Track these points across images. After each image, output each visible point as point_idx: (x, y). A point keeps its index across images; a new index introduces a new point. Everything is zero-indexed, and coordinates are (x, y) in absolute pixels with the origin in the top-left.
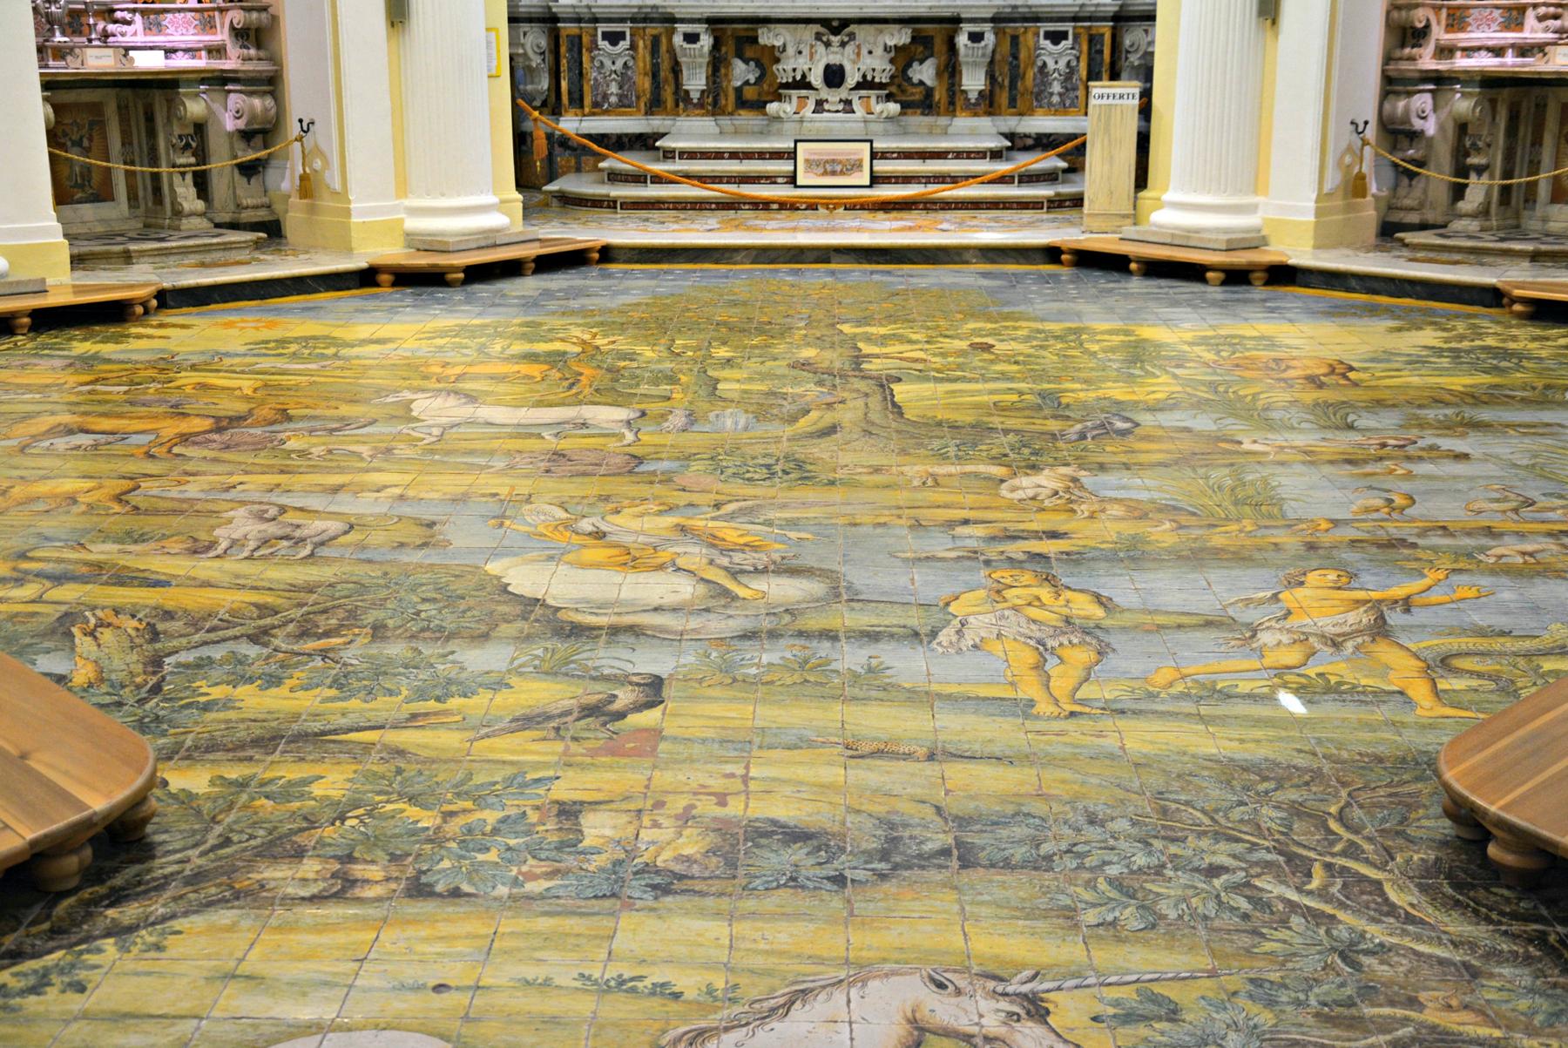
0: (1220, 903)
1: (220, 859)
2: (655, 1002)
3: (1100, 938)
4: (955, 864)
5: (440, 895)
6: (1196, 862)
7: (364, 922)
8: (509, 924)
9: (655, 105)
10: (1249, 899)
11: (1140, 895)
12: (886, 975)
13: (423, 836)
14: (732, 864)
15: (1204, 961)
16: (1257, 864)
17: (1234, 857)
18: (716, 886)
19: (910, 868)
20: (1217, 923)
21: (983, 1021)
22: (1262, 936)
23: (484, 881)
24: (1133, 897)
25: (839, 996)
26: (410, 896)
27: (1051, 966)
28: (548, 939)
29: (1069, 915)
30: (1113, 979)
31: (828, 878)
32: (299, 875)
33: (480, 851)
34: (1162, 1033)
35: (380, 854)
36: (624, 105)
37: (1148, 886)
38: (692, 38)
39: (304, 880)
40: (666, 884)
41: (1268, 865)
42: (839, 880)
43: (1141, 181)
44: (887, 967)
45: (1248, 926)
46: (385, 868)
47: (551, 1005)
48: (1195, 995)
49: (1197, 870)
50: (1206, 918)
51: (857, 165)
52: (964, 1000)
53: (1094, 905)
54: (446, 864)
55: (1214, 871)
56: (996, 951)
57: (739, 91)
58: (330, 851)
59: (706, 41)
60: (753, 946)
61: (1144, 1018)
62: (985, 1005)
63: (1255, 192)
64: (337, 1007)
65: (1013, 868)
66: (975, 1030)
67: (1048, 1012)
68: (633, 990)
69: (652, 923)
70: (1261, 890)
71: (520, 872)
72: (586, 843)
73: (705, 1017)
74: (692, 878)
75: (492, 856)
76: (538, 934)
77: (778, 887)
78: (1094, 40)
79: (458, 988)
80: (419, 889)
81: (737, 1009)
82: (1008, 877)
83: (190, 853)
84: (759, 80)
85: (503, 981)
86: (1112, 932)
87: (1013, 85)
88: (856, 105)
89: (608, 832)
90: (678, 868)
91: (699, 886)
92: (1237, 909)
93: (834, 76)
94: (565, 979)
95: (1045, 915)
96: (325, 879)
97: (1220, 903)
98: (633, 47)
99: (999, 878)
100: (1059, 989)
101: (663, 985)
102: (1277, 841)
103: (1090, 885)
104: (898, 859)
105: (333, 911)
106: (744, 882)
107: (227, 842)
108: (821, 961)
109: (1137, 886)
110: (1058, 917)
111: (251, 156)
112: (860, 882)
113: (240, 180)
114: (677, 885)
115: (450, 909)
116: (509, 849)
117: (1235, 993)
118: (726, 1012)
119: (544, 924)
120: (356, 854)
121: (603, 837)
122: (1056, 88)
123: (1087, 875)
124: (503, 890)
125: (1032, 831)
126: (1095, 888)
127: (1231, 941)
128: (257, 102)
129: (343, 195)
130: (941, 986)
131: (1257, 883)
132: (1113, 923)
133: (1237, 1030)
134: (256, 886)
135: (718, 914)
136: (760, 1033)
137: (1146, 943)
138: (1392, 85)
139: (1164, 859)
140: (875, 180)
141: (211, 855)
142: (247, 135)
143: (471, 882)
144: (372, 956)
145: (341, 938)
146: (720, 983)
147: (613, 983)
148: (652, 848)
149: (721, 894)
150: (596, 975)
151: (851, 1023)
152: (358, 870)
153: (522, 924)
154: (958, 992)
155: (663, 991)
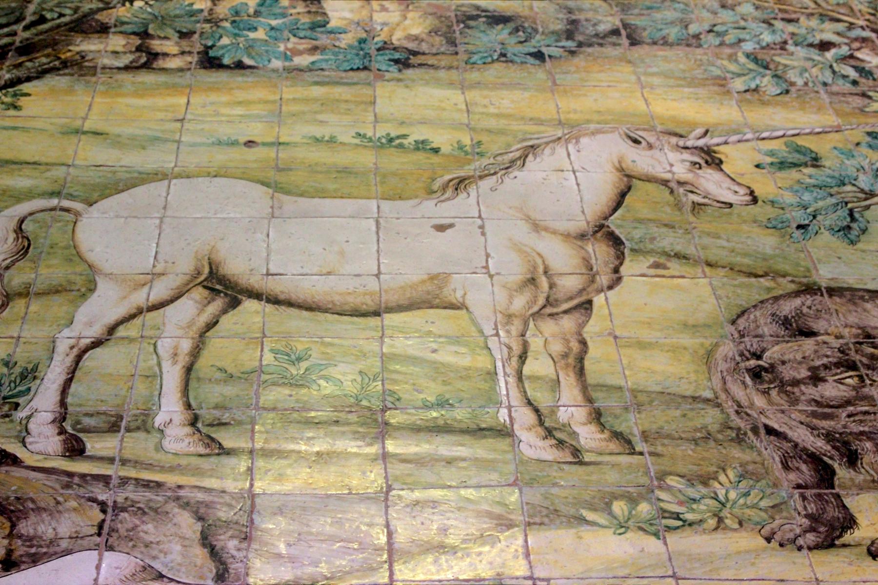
0: (834, 72)
1: (41, 33)
2: (420, 156)
3: (749, 102)
4: (625, 41)
5: (228, 67)
6: (810, 40)
7: (174, 88)
8: (289, 92)
10: (855, 68)
11: (772, 66)
12: (593, 134)
13: (201, 17)
14: (452, 42)
15: (831, 119)
16: (856, 39)
17: (838, 34)
18: (444, 61)
19: (590, 45)
20: (835, 89)
21: (674, 169)
22: (870, 97)
23: (260, 55)
24: (767, 67)
25: (561, 151)
26: (205, 68)
27: (717, 125)
28: (326, 104)
29: (721, 83)
30: (764, 135)
31: (531, 54)
32: (110, 48)
33: (249, 29)
34: (810, 177)
35: (170, 32)
37: (777, 59)
39: (115, 53)
40: (405, 59)
41: (864, 40)
42: (539, 56)
44: (592, 126)
45: (857, 90)
46: (177, 44)
47: (342, 158)
48: (828, 146)
49: (811, 45)
50: (825, 84)
52: (656, 153)
53: (739, 75)
54: (225, 41)
55: (824, 46)
56: (672, 113)
58: (128, 28)
60: (485, 110)
61: (795, 165)
62: (674, 156)
64: (173, 158)
65: (671, 45)
66: (668, 176)
67: (721, 162)
68: (401, 146)
69: (401, 92)
70: (862, 61)
71: (287, 49)
72: (333, 24)
73: (461, 167)
74: (424, 54)
75: (260, 34)
76: (315, 100)
77: (493, 61)
79: (264, 144)
80: (210, 62)
81: (485, 161)
82: (668, 52)
83: (14, 27)
85: (297, 139)
86: (756, 96)
89: (348, 15)
90: (412, 46)
91: (431, 61)
92: (847, 77)
94: (346, 137)
95: (702, 83)
96: (131, 52)
97: (834, 72)
99: (661, 53)
100: (726, 143)
101: (423, 142)
102: (868, 20)
103: (732, 58)
104: (580, 38)
105: (146, 78)
106: (465, 57)
107: (42, 20)
108: (540, 122)
109: (768, 60)
110: (714, 85)
112: (556, 58)
114: (413, 60)
115: (240, 79)
116: (272, 28)
117: (858, 144)
118: (477, 163)
119: (317, 91)
120: (151, 31)
121: (345, 19)
123: (728, 51)
124: (277, 64)
125: (680, 15)
126: (736, 61)
127: (848, 103)
130: (636, 142)
131: (858, 55)
132: (756, 90)
133: (865, 173)
134: (78, 57)
135: (451, 84)
136: (507, 180)
137: (785, 105)
139: (785, 36)
141: (33, 31)
143: (249, 56)
144: (189, 116)
145: (160, 102)
146: (467, 141)
147: (384, 141)
148: (386, 29)
149: (450, 68)
150: (370, 134)
151: (574, 172)
152: (157, 45)
153: (300, 92)
154: (650, 146)
155: (421, 146)
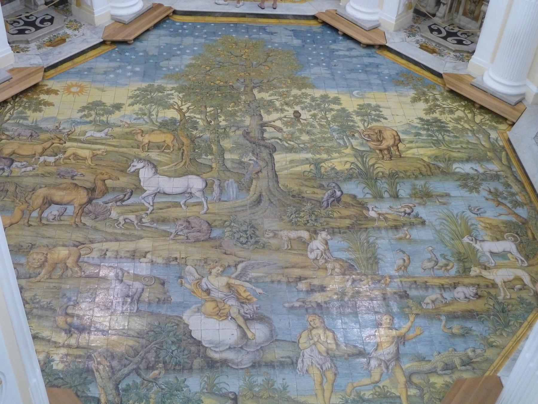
129: (91, 7)
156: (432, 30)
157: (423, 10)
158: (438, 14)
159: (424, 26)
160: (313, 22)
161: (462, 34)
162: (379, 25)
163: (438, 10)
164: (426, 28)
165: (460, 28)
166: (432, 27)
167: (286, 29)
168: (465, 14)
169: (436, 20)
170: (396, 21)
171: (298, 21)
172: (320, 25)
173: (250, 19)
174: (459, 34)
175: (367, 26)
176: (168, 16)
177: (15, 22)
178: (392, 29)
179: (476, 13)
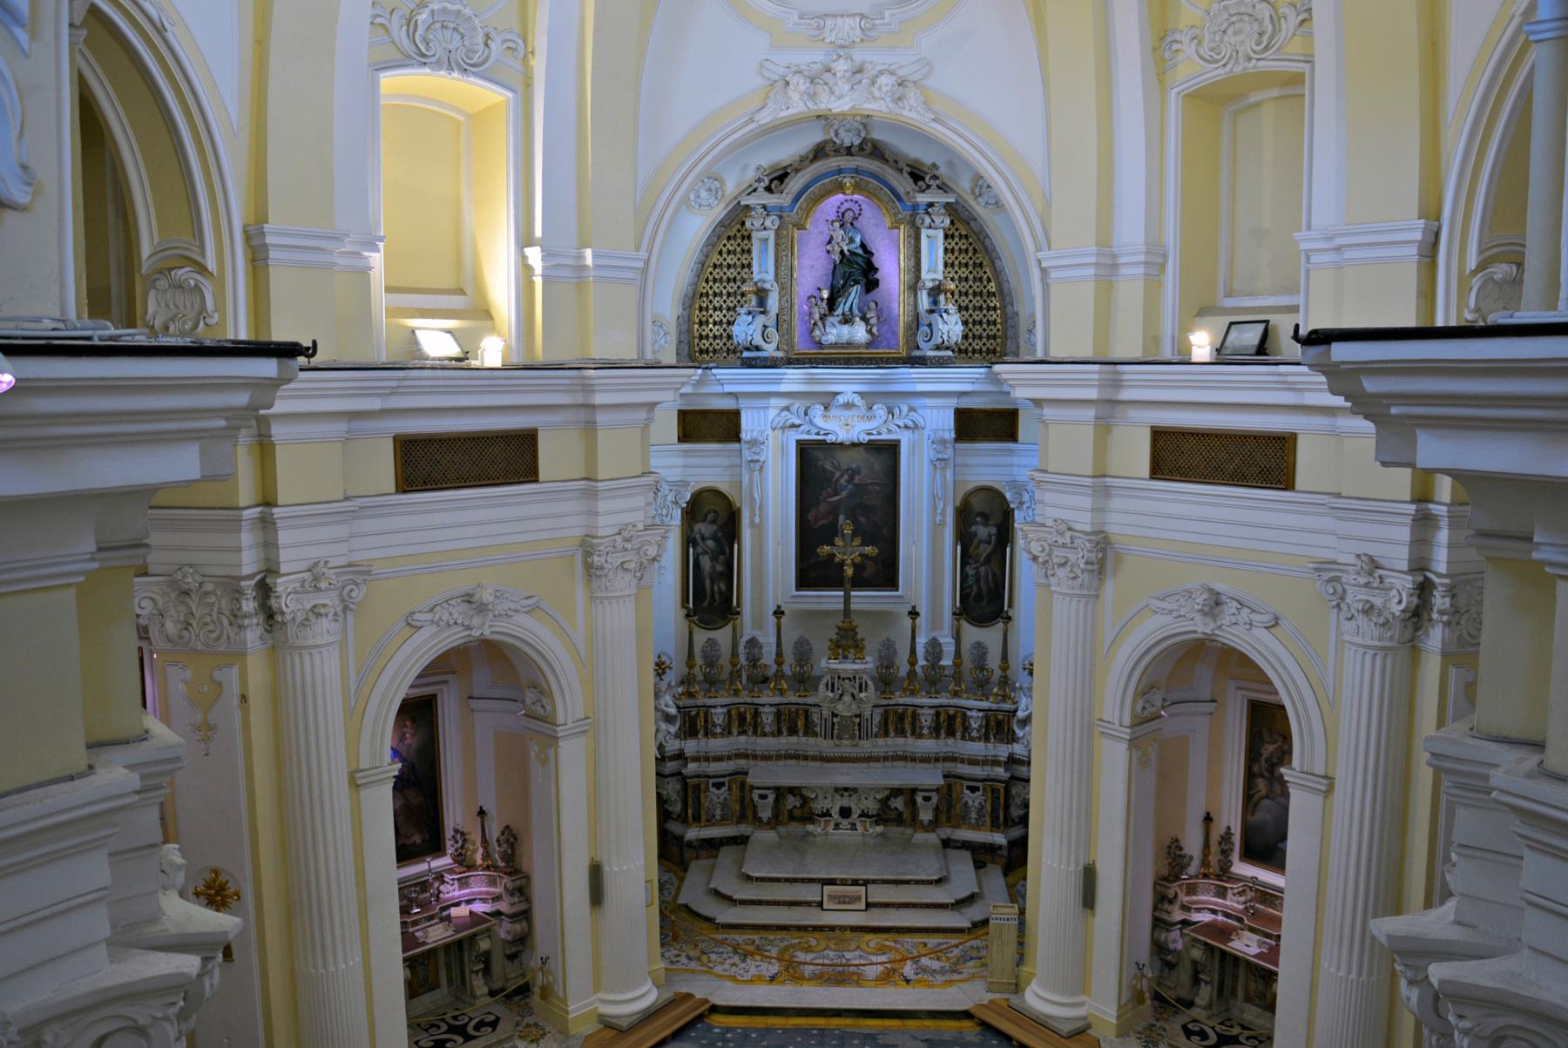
9: (742, 818)
36: (724, 819)
38: (763, 797)
43: (1021, 959)
51: (858, 899)
57: (790, 812)
59: (771, 798)
63: (1083, 993)
78: (994, 791)
84: (802, 806)
87: (948, 811)
88: (859, 826)
93: (845, 812)
98: (730, 788)
111: (514, 950)
113: (508, 964)
122: (974, 815)
128: (518, 927)
129: (564, 1001)
138: (1159, 923)
140: (869, 905)
142: (512, 943)
156: (1188, 1033)
157: (1169, 995)
158: (1198, 1000)
159: (1174, 1027)
160: (966, 1024)
161: (1248, 1038)
162: (1089, 1026)
163: (1197, 994)
164: (1178, 1027)
165: (1244, 1027)
166: (1190, 1026)
167: (915, 1038)
168: (1248, 999)
169: (1195, 1012)
170: (1118, 1017)
171: (938, 1023)
172: (978, 1029)
173: (848, 1021)
174: (1242, 1039)
175: (1066, 1028)
176: (700, 1018)
177: (433, 1026)
178: (1112, 1036)
179: (1269, 996)
